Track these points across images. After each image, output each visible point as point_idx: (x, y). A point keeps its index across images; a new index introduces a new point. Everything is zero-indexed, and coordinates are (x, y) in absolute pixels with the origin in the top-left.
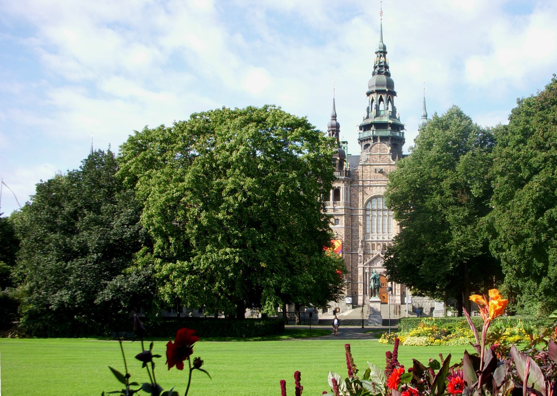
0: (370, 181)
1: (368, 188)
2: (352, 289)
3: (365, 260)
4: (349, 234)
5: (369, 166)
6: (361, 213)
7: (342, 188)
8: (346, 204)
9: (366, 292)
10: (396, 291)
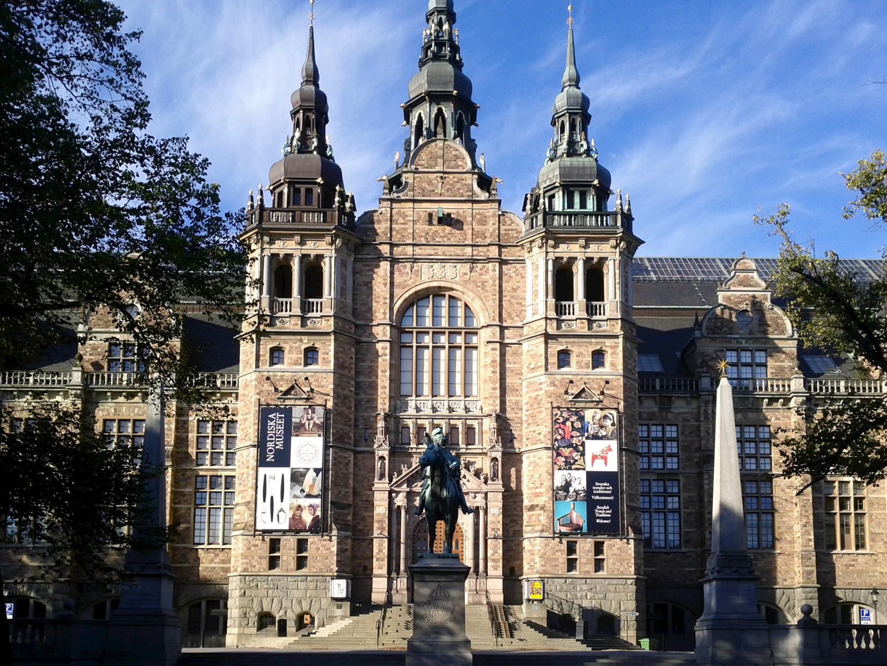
0: (414, 245)
1: (408, 265)
2: (354, 557)
3: (394, 469)
4: (346, 392)
5: (411, 205)
6: (384, 334)
7: (327, 260)
8: (340, 306)
9: (398, 565)
10: (490, 564)
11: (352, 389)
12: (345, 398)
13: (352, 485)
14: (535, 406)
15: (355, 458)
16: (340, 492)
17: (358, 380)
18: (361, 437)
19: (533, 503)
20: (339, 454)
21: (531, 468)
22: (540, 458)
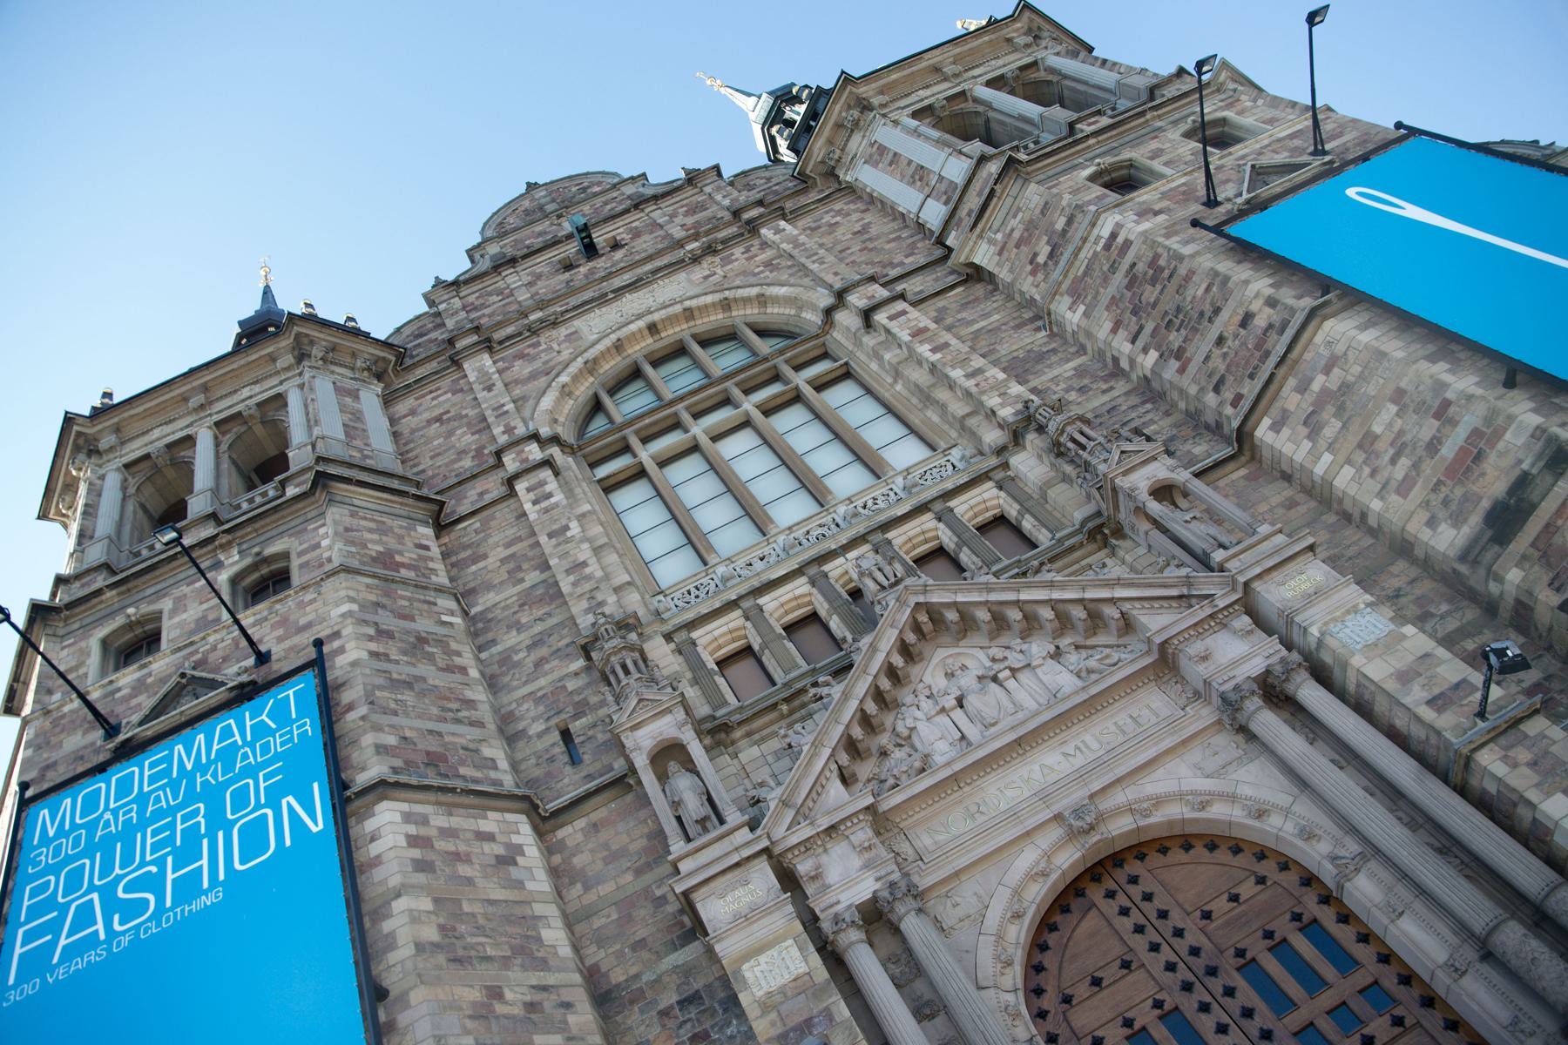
4: (423, 625)
11: (445, 618)
12: (422, 640)
13: (565, 951)
14: (1150, 294)
15: (549, 850)
16: (496, 993)
17: (473, 611)
18: (552, 760)
19: (1486, 504)
20: (439, 820)
21: (1331, 429)
22: (1327, 371)
